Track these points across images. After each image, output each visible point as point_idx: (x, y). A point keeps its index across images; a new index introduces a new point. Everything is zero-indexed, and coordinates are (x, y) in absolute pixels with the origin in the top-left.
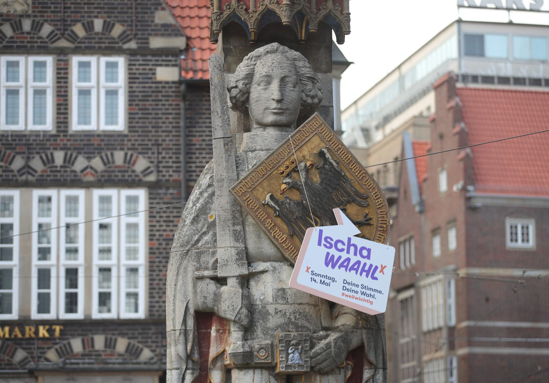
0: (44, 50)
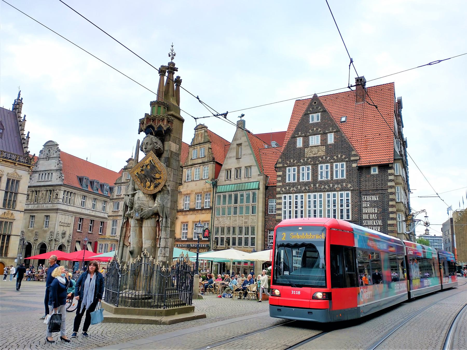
0: (328, 162)
